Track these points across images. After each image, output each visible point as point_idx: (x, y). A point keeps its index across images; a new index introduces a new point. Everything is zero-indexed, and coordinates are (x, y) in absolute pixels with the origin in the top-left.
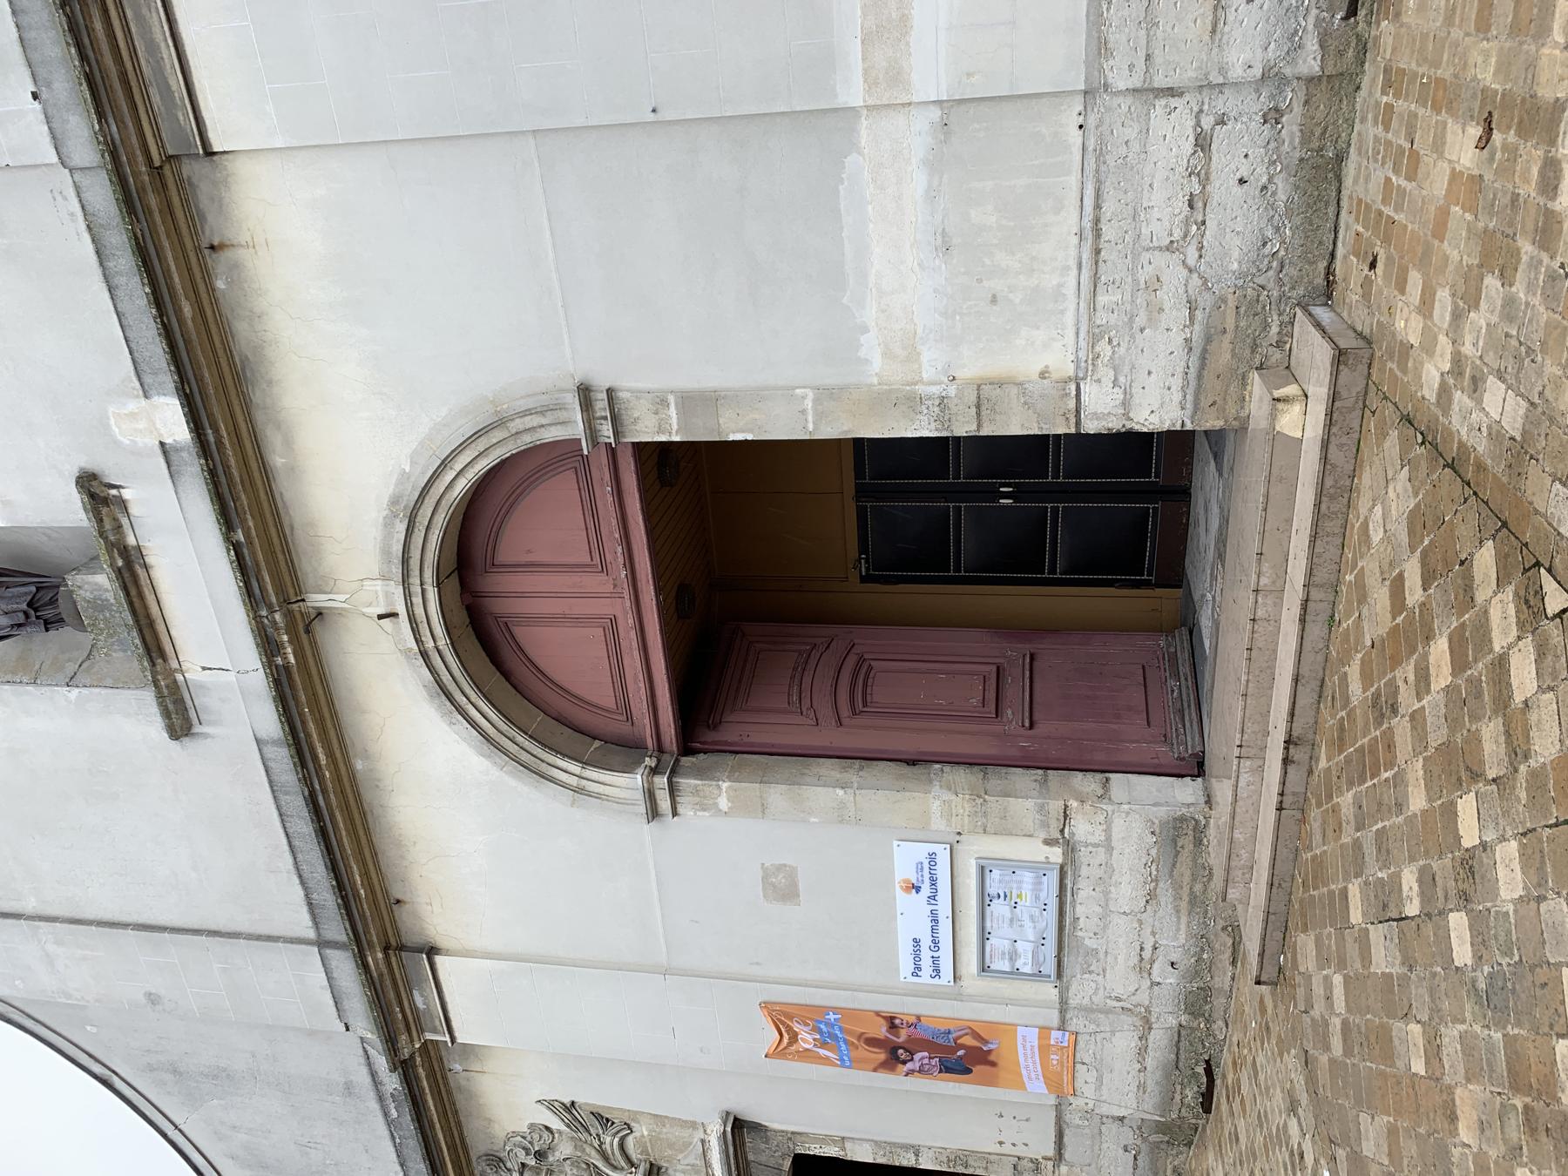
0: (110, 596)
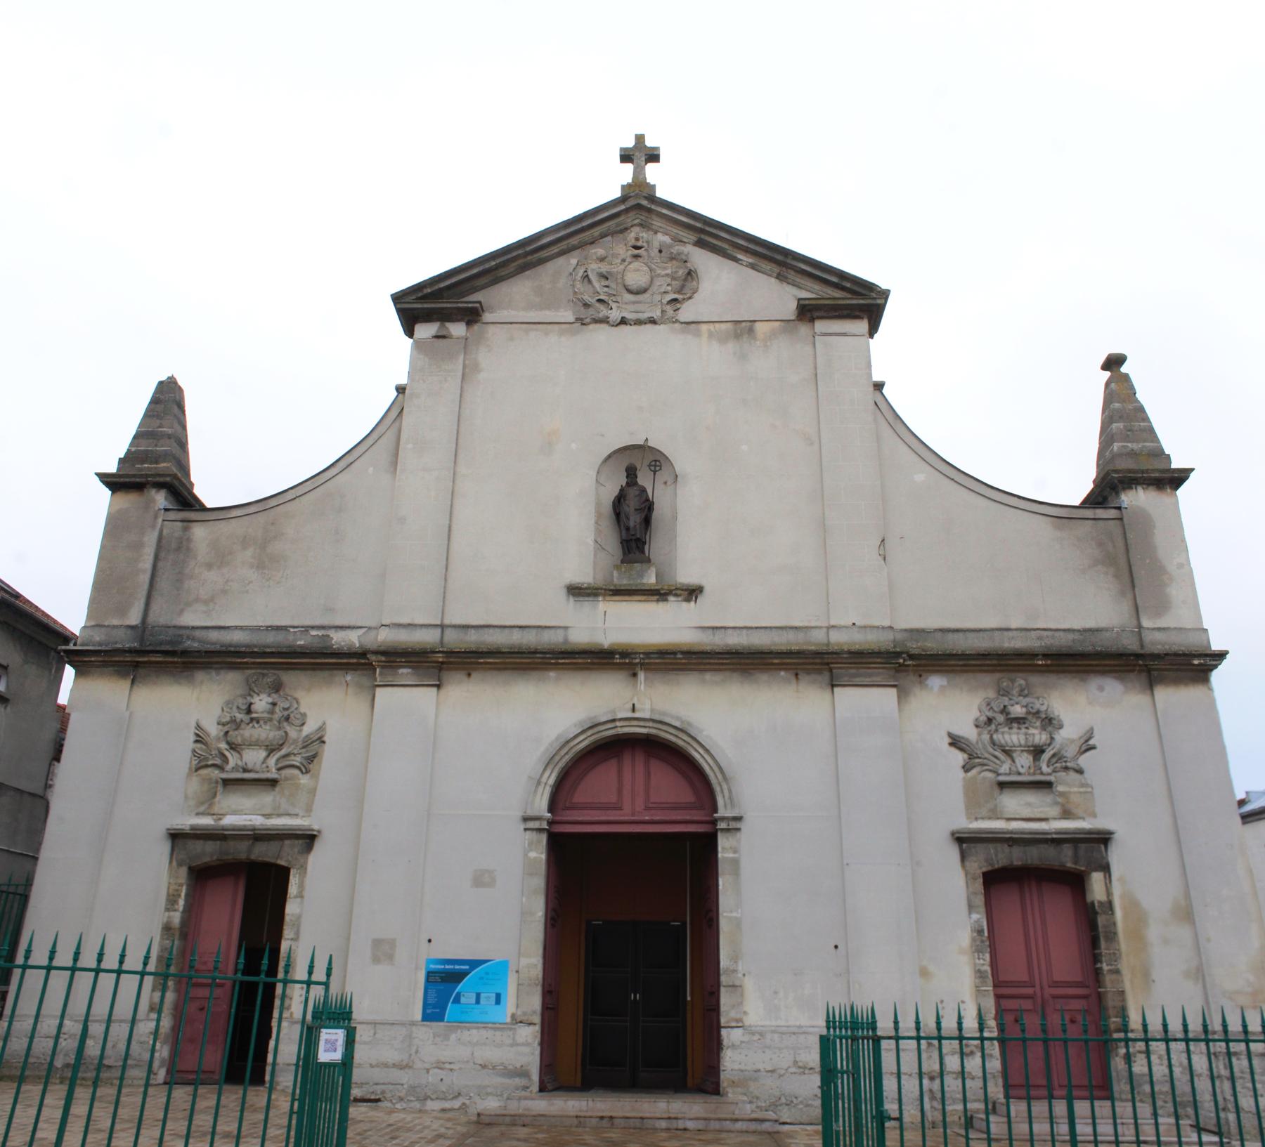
0: (645, 581)
